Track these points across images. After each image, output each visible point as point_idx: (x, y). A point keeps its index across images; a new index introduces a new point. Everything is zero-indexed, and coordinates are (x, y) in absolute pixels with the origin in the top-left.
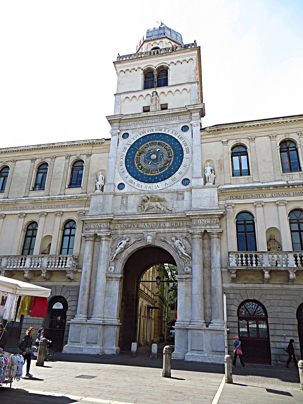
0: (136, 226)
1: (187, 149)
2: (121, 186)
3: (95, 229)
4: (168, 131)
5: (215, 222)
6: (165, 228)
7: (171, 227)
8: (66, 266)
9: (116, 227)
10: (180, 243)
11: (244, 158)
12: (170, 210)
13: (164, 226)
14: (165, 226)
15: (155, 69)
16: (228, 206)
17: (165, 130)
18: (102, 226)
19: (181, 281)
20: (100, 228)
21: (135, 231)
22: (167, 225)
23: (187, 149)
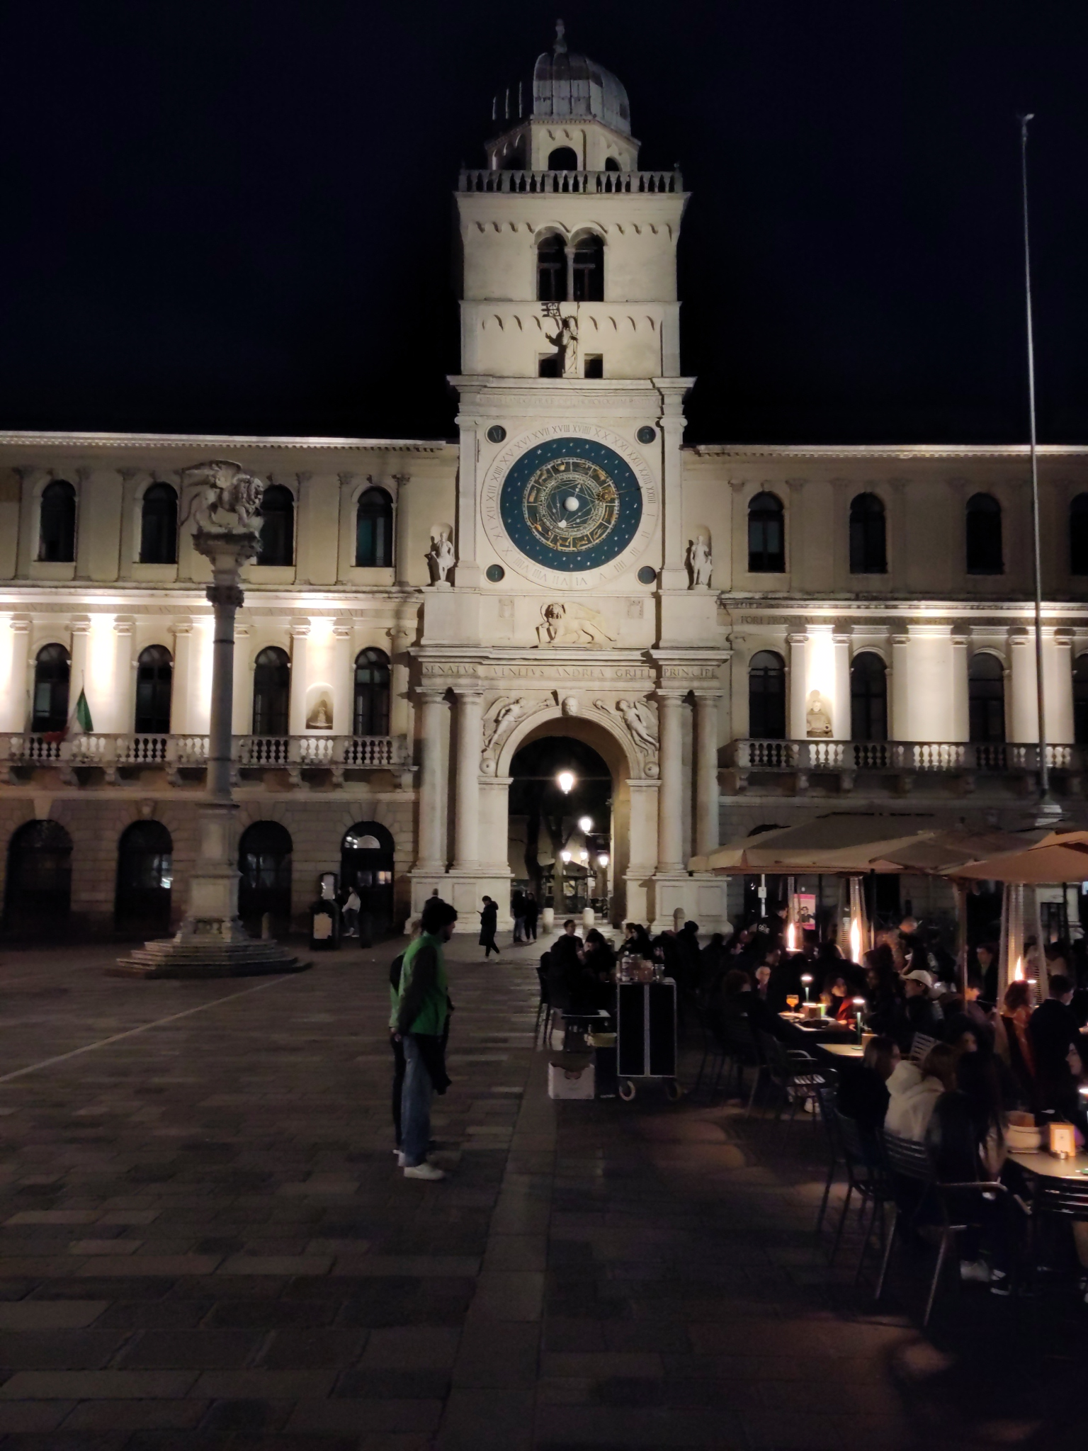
0: (538, 673)
1: (651, 491)
2: (496, 573)
3: (446, 676)
4: (606, 436)
5: (710, 674)
6: (603, 679)
7: (619, 678)
8: (392, 761)
9: (493, 674)
10: (638, 716)
11: (773, 526)
12: (612, 639)
13: (600, 675)
14: (603, 675)
15: (570, 235)
16: (736, 638)
17: (597, 433)
18: (462, 671)
19: (638, 791)
20: (458, 676)
21: (536, 684)
22: (609, 672)
23: (651, 491)
